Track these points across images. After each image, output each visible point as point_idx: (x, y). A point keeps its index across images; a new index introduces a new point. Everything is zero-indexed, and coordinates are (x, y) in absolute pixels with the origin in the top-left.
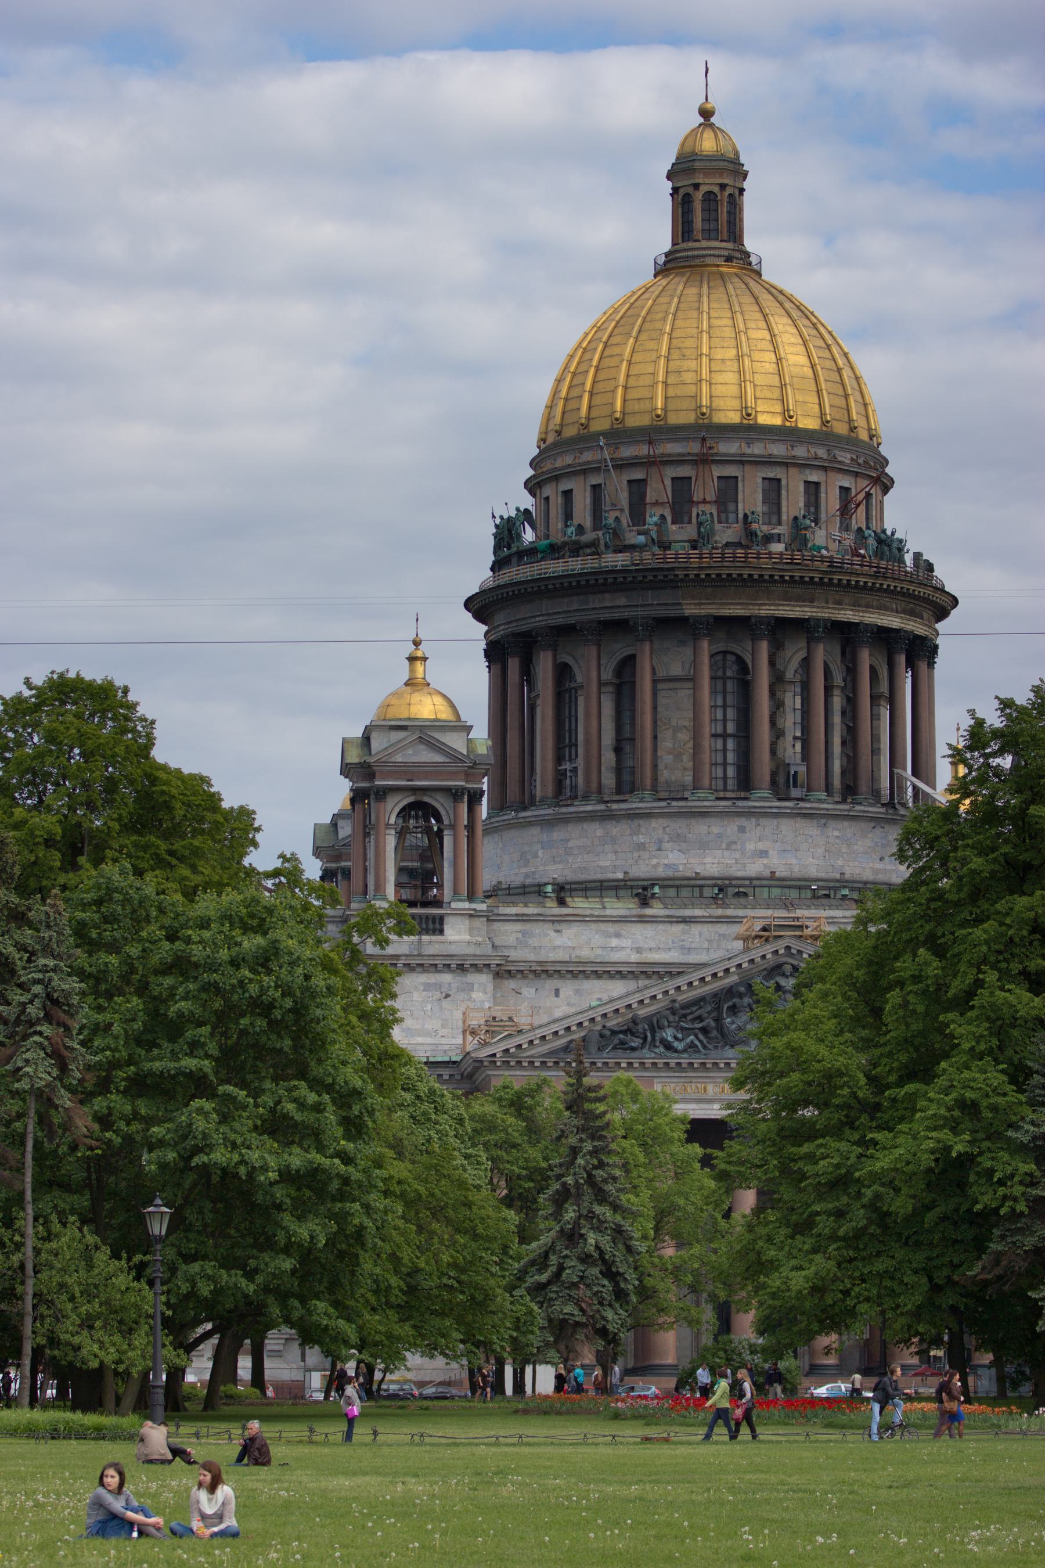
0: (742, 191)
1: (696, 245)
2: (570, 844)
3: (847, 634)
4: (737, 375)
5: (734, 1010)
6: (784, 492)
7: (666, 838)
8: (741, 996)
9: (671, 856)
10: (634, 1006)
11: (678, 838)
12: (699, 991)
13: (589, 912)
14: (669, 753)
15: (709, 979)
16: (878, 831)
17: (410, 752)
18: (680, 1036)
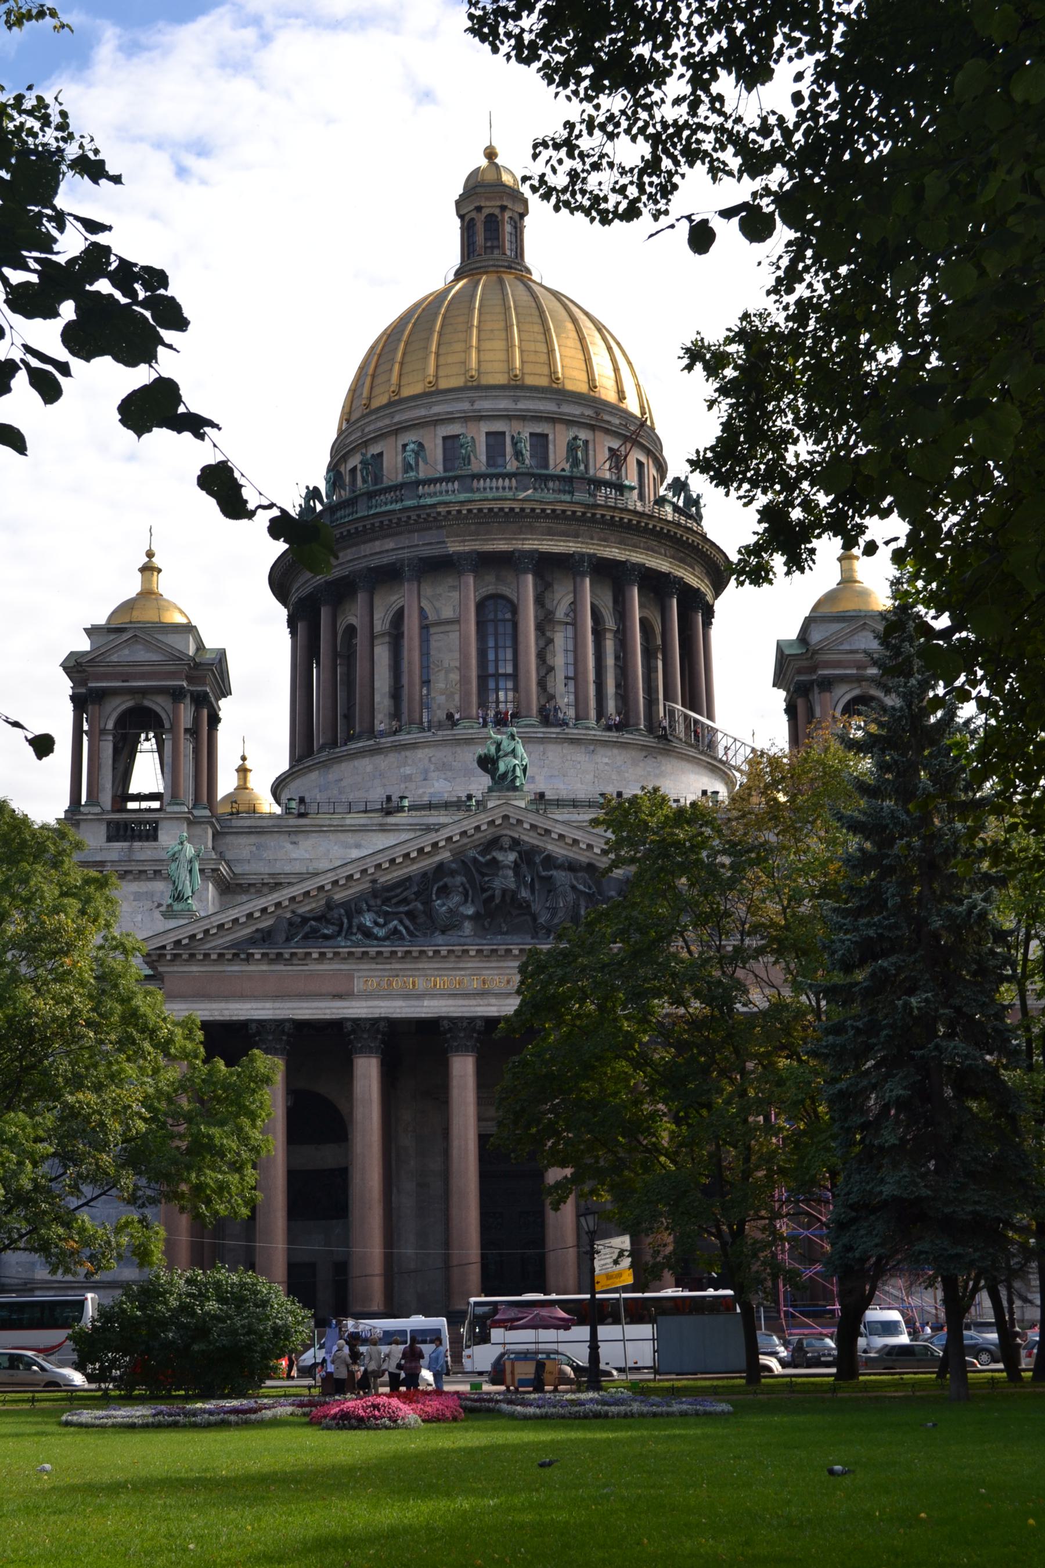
0: (522, 216)
1: (479, 258)
2: (344, 783)
3: (613, 575)
4: (504, 343)
5: (444, 891)
6: (551, 446)
7: (432, 767)
8: (453, 873)
9: (436, 784)
10: (328, 887)
11: (444, 767)
12: (406, 870)
13: (327, 822)
14: (442, 694)
15: (414, 855)
16: (650, 761)
17: (126, 652)
18: (381, 921)
